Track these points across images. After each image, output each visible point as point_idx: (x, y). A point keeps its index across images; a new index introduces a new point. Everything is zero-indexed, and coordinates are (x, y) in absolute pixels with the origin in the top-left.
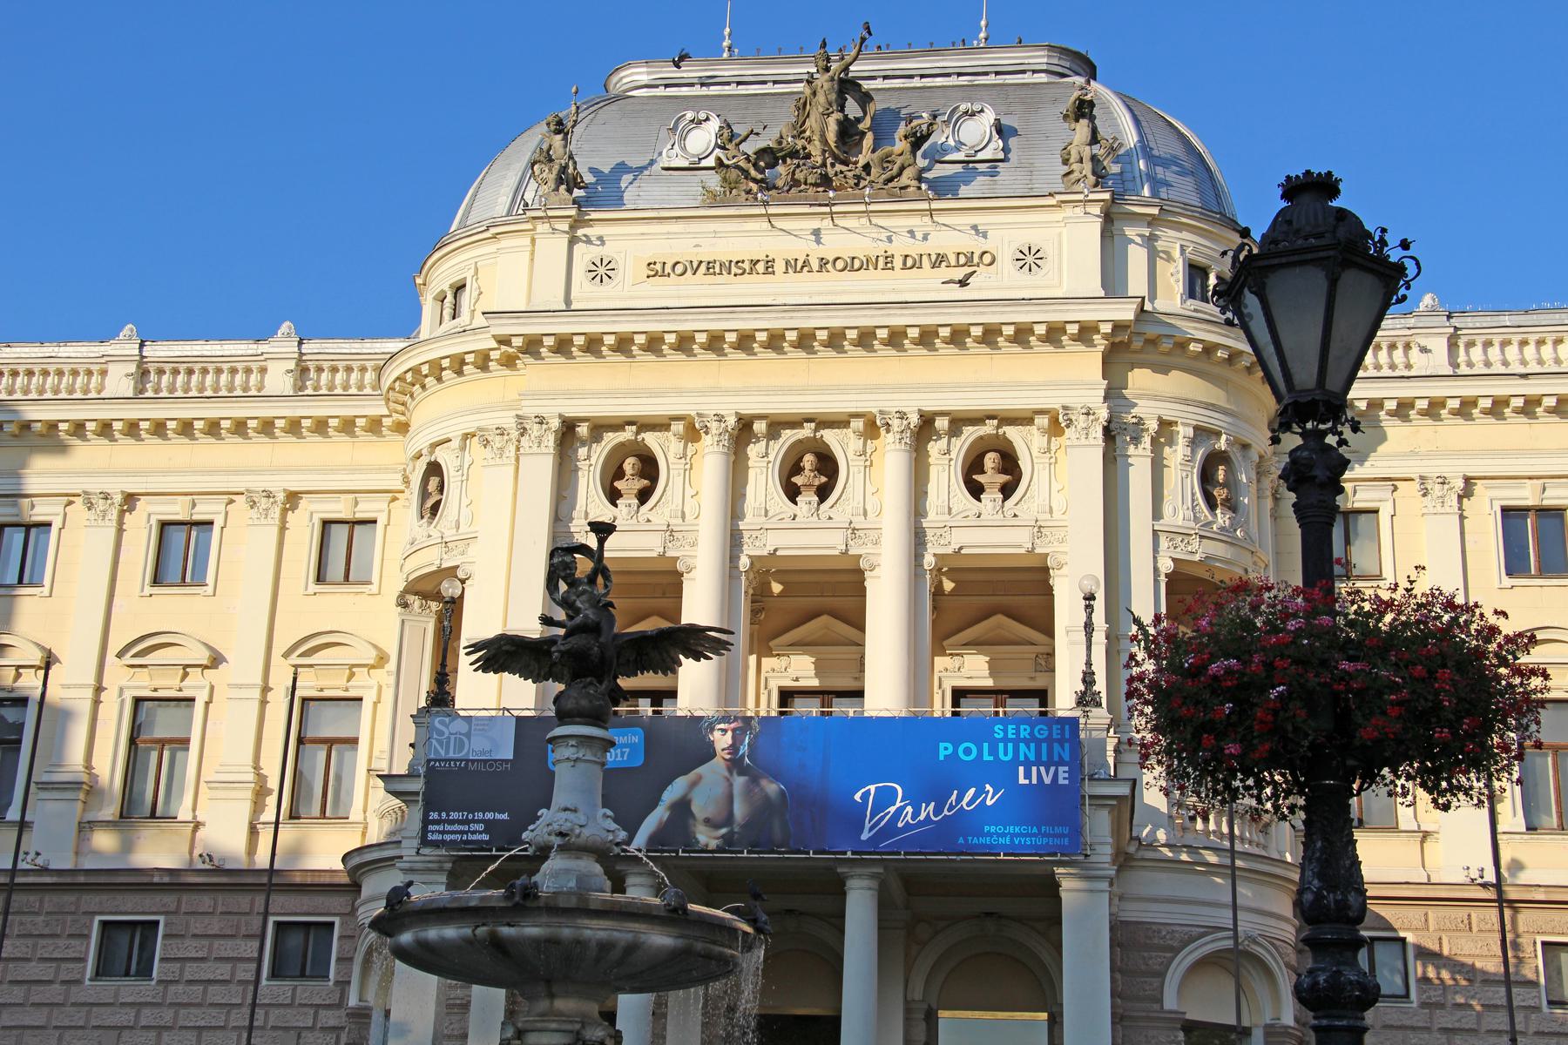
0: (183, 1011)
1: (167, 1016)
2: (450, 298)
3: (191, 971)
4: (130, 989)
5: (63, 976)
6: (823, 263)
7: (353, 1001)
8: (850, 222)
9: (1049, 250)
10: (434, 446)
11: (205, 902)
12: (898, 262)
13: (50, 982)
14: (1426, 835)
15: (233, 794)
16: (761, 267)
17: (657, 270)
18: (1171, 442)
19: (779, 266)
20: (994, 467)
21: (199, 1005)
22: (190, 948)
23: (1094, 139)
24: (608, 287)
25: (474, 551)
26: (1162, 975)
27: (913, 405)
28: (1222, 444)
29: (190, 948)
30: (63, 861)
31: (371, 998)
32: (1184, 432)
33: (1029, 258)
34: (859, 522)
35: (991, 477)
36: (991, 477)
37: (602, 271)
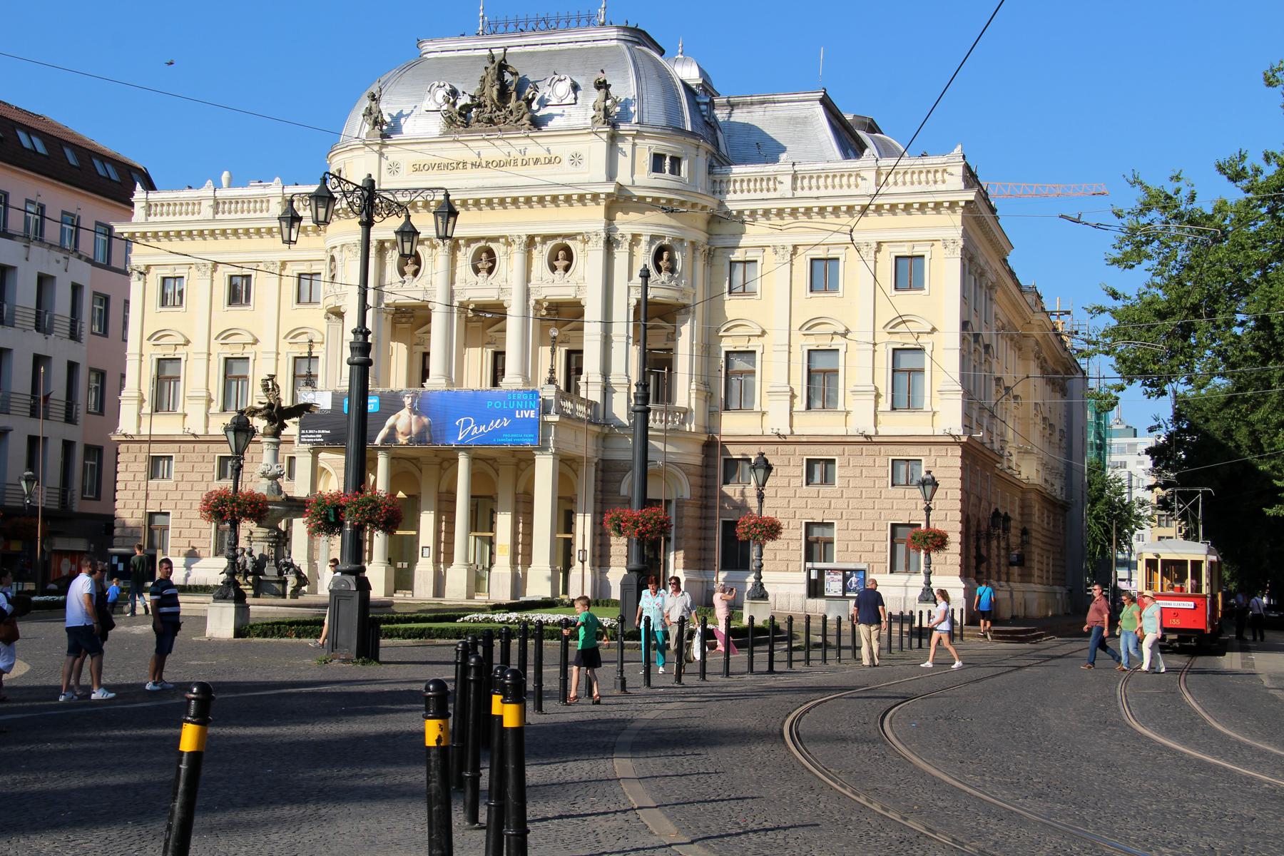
8: (498, 143)
9: (585, 156)
12: (519, 162)
14: (764, 413)
17: (417, 168)
18: (638, 244)
20: (562, 256)
23: (607, 98)
24: (397, 177)
26: (620, 482)
27: (525, 231)
28: (666, 242)
30: (200, 431)
32: (644, 240)
33: (576, 159)
34: (504, 285)
35: (561, 264)
36: (561, 264)
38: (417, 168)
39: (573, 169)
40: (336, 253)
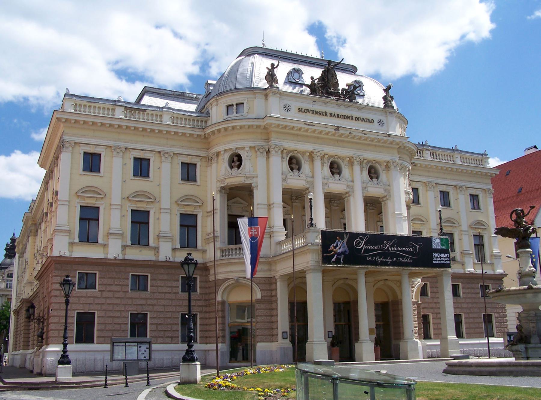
0: (159, 301)
1: (155, 302)
2: (235, 106)
3: (160, 289)
4: (143, 294)
5: (123, 290)
6: (338, 115)
7: (219, 298)
9: (385, 122)
10: (236, 148)
11: (162, 271)
13: (119, 291)
15: (167, 240)
16: (324, 114)
17: (300, 110)
19: (328, 115)
21: (163, 299)
22: (159, 283)
24: (289, 113)
25: (255, 179)
29: (159, 283)
31: (225, 298)
37: (287, 108)
38: (300, 110)
39: (379, 127)
40: (241, 153)
